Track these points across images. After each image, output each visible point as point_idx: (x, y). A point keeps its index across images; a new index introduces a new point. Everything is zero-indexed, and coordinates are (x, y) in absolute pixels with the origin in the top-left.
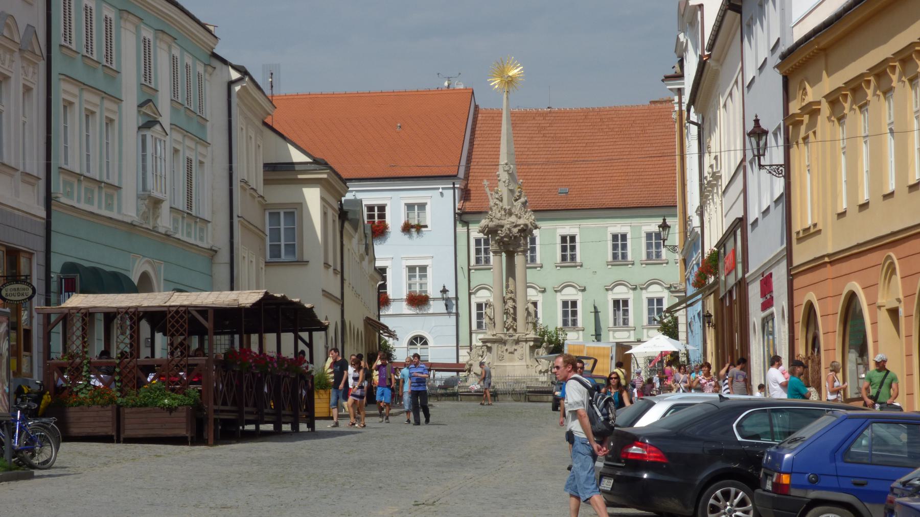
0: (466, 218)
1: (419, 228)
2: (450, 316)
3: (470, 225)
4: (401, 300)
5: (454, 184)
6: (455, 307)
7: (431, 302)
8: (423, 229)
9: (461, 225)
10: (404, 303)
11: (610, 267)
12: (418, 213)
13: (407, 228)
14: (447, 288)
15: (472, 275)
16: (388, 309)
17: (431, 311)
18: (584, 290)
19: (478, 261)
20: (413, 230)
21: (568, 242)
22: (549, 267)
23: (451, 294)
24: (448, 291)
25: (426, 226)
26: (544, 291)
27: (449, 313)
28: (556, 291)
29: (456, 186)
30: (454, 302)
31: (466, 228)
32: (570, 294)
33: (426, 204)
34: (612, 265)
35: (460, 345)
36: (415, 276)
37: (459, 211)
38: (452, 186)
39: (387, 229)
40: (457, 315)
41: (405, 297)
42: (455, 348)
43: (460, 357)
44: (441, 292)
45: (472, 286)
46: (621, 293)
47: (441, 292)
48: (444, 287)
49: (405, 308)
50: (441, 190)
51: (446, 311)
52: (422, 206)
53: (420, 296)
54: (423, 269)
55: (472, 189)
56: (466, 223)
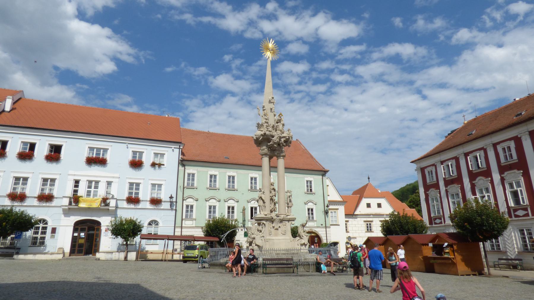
0: (185, 163)
1: (160, 165)
2: (172, 210)
3: (186, 167)
4: (146, 201)
5: (180, 146)
6: (175, 206)
7: (163, 203)
8: (162, 166)
9: (181, 166)
10: (148, 203)
11: (249, 192)
12: (160, 158)
13: (153, 165)
14: (173, 196)
15: (184, 190)
16: (139, 205)
17: (162, 208)
18: (238, 202)
19: (188, 184)
20: (157, 166)
21: (231, 179)
22: (222, 190)
23: (174, 200)
24: (173, 197)
25: (163, 165)
26: (219, 201)
27: (172, 209)
28: (225, 201)
29: (181, 147)
30: (175, 203)
31: (184, 168)
32: (231, 203)
33: (164, 154)
34: (251, 191)
35: (176, 226)
36: (155, 190)
37: (181, 159)
38: (179, 147)
39: (143, 164)
40: (176, 210)
41: (149, 199)
42: (174, 227)
43: (175, 232)
44: (170, 197)
45: (184, 196)
47: (170, 197)
48: (171, 195)
49: (148, 205)
50: (173, 148)
51: (170, 208)
52: (162, 155)
53: (157, 199)
54: (160, 186)
55: (184, 152)
56: (184, 165)
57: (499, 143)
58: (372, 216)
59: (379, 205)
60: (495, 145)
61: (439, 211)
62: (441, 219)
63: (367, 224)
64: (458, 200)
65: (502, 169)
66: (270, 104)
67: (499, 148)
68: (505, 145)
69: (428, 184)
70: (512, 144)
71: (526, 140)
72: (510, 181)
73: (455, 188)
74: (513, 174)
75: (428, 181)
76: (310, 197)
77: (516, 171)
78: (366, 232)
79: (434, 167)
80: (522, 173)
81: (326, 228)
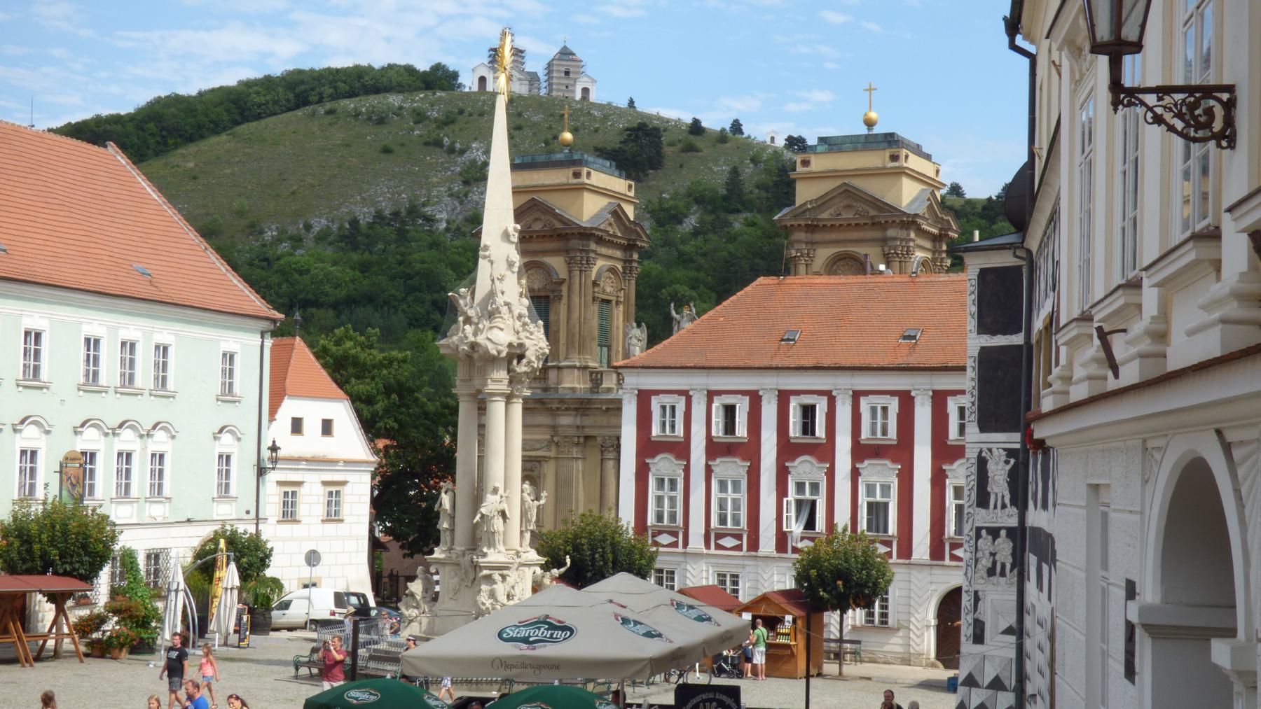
46: (90, 440)
57: (866, 393)
58: (304, 467)
59: (327, 427)
60: (857, 396)
61: (673, 517)
62: (675, 534)
63: (286, 494)
64: (736, 496)
65: (861, 452)
66: (506, 244)
67: (865, 404)
68: (880, 401)
69: (653, 439)
70: (894, 405)
71: (923, 405)
72: (872, 479)
73: (732, 469)
74: (879, 468)
75: (656, 431)
76: (228, 414)
77: (888, 462)
78: (278, 522)
79: (683, 399)
80: (899, 470)
81: (257, 525)
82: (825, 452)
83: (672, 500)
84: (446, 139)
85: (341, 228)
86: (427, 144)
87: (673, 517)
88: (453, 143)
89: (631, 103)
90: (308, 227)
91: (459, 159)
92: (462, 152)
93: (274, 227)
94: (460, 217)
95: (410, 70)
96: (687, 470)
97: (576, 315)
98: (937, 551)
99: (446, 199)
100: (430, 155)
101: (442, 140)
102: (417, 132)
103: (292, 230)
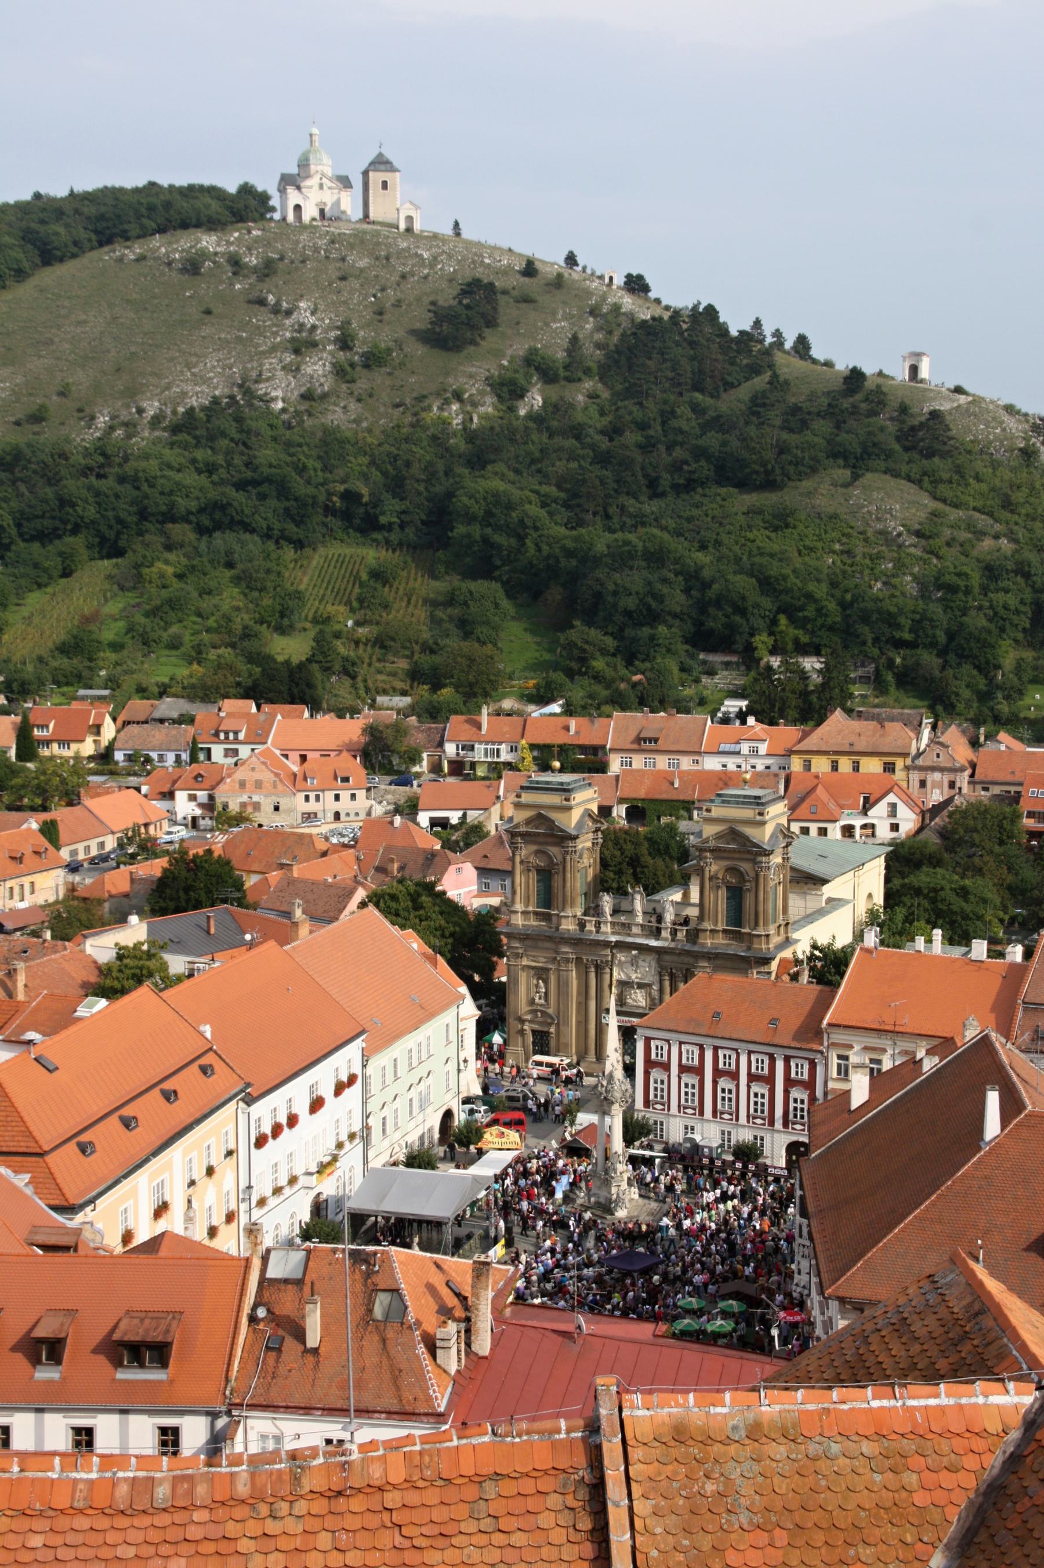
61: (662, 1097)
65: (752, 1078)
82: (735, 1076)
83: (662, 1090)
84: (271, 297)
85: (174, 412)
86: (249, 302)
87: (662, 1097)
88: (278, 303)
89: (457, 225)
90: (140, 411)
91: (287, 322)
92: (289, 313)
93: (106, 412)
94: (296, 393)
95: (213, 191)
96: (669, 1077)
97: (568, 884)
98: (786, 1124)
99: (280, 374)
100: (256, 316)
101: (266, 299)
102: (238, 286)
103: (124, 416)
